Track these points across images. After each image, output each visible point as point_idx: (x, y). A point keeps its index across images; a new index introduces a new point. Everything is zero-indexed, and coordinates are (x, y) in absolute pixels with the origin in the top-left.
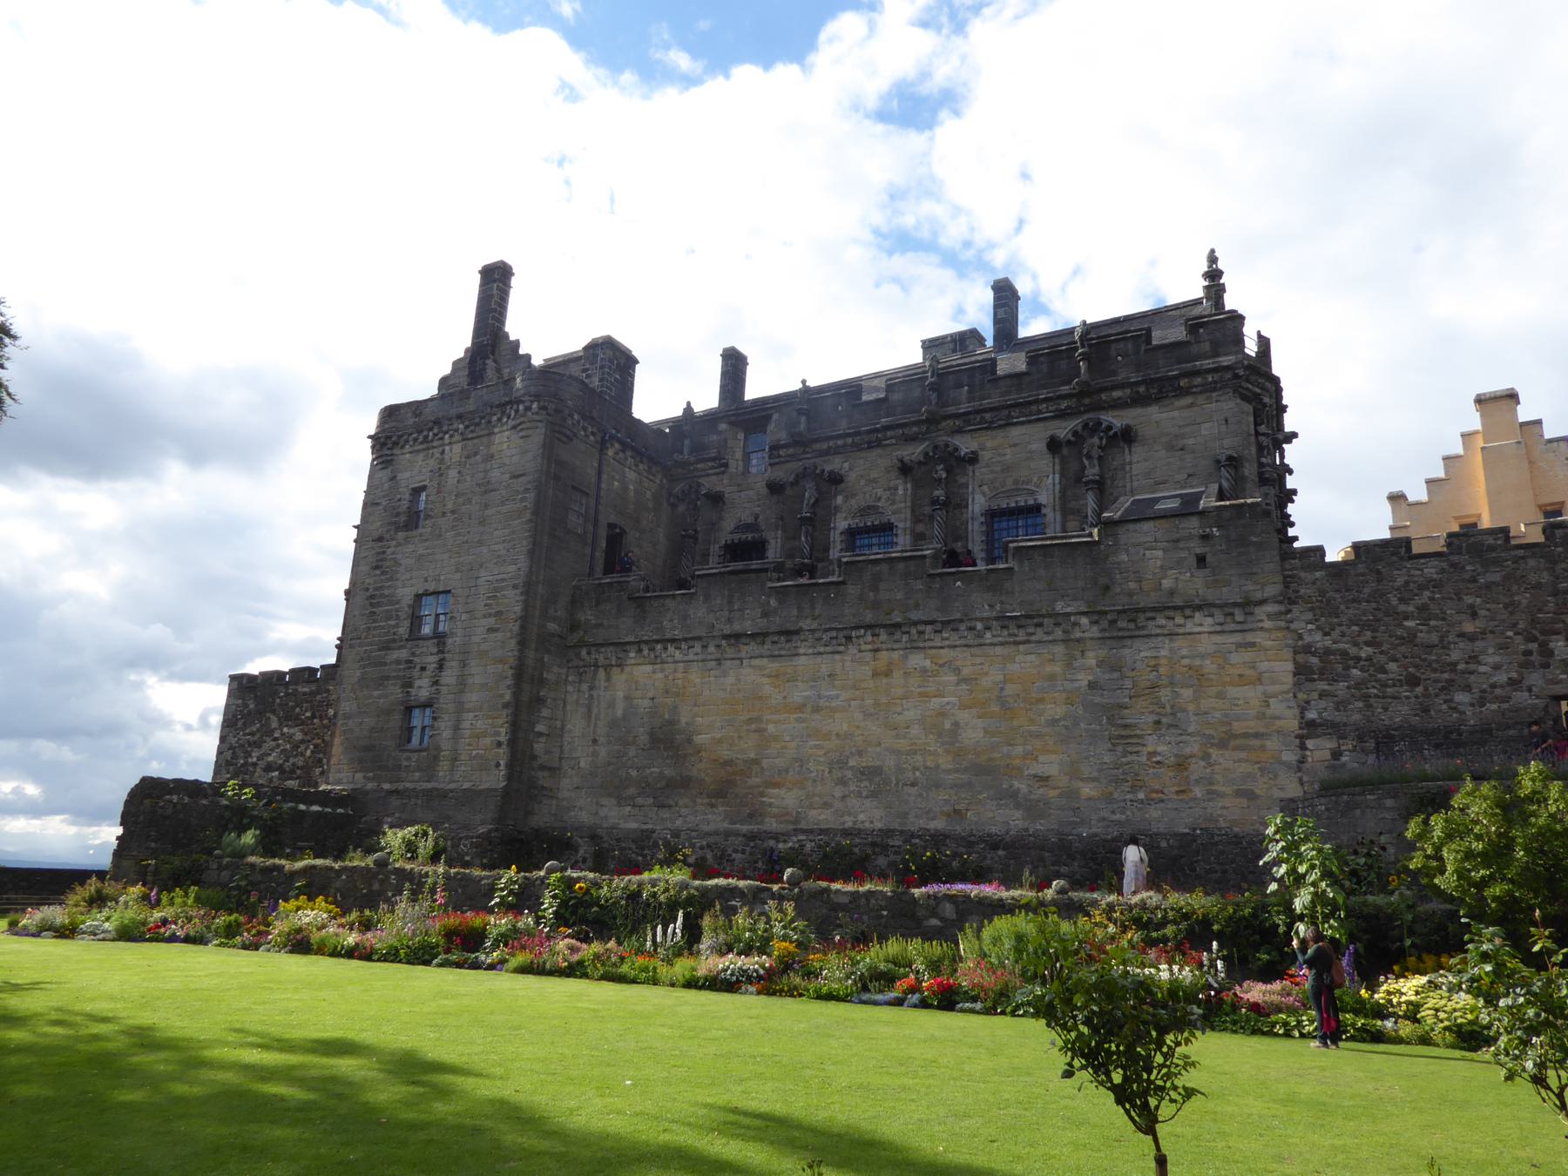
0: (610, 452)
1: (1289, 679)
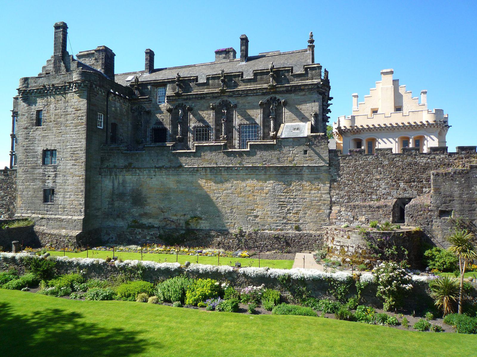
0: (110, 98)
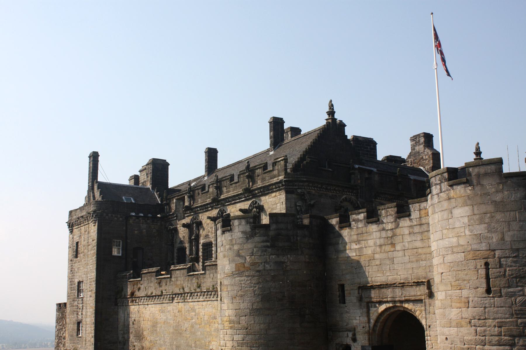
0: (131, 221)
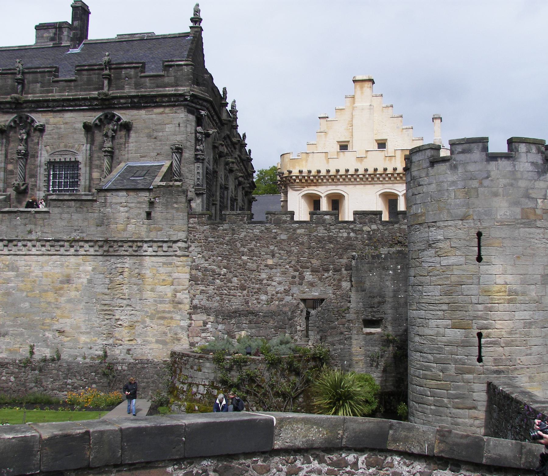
1: (187, 283)
